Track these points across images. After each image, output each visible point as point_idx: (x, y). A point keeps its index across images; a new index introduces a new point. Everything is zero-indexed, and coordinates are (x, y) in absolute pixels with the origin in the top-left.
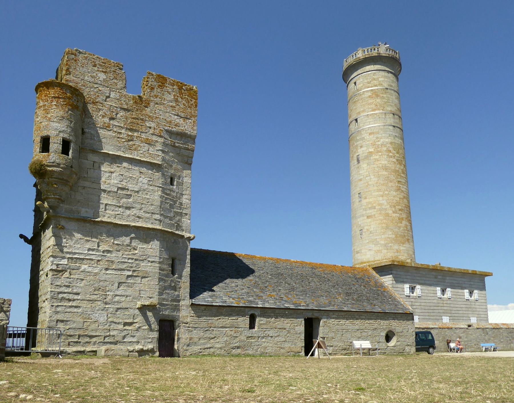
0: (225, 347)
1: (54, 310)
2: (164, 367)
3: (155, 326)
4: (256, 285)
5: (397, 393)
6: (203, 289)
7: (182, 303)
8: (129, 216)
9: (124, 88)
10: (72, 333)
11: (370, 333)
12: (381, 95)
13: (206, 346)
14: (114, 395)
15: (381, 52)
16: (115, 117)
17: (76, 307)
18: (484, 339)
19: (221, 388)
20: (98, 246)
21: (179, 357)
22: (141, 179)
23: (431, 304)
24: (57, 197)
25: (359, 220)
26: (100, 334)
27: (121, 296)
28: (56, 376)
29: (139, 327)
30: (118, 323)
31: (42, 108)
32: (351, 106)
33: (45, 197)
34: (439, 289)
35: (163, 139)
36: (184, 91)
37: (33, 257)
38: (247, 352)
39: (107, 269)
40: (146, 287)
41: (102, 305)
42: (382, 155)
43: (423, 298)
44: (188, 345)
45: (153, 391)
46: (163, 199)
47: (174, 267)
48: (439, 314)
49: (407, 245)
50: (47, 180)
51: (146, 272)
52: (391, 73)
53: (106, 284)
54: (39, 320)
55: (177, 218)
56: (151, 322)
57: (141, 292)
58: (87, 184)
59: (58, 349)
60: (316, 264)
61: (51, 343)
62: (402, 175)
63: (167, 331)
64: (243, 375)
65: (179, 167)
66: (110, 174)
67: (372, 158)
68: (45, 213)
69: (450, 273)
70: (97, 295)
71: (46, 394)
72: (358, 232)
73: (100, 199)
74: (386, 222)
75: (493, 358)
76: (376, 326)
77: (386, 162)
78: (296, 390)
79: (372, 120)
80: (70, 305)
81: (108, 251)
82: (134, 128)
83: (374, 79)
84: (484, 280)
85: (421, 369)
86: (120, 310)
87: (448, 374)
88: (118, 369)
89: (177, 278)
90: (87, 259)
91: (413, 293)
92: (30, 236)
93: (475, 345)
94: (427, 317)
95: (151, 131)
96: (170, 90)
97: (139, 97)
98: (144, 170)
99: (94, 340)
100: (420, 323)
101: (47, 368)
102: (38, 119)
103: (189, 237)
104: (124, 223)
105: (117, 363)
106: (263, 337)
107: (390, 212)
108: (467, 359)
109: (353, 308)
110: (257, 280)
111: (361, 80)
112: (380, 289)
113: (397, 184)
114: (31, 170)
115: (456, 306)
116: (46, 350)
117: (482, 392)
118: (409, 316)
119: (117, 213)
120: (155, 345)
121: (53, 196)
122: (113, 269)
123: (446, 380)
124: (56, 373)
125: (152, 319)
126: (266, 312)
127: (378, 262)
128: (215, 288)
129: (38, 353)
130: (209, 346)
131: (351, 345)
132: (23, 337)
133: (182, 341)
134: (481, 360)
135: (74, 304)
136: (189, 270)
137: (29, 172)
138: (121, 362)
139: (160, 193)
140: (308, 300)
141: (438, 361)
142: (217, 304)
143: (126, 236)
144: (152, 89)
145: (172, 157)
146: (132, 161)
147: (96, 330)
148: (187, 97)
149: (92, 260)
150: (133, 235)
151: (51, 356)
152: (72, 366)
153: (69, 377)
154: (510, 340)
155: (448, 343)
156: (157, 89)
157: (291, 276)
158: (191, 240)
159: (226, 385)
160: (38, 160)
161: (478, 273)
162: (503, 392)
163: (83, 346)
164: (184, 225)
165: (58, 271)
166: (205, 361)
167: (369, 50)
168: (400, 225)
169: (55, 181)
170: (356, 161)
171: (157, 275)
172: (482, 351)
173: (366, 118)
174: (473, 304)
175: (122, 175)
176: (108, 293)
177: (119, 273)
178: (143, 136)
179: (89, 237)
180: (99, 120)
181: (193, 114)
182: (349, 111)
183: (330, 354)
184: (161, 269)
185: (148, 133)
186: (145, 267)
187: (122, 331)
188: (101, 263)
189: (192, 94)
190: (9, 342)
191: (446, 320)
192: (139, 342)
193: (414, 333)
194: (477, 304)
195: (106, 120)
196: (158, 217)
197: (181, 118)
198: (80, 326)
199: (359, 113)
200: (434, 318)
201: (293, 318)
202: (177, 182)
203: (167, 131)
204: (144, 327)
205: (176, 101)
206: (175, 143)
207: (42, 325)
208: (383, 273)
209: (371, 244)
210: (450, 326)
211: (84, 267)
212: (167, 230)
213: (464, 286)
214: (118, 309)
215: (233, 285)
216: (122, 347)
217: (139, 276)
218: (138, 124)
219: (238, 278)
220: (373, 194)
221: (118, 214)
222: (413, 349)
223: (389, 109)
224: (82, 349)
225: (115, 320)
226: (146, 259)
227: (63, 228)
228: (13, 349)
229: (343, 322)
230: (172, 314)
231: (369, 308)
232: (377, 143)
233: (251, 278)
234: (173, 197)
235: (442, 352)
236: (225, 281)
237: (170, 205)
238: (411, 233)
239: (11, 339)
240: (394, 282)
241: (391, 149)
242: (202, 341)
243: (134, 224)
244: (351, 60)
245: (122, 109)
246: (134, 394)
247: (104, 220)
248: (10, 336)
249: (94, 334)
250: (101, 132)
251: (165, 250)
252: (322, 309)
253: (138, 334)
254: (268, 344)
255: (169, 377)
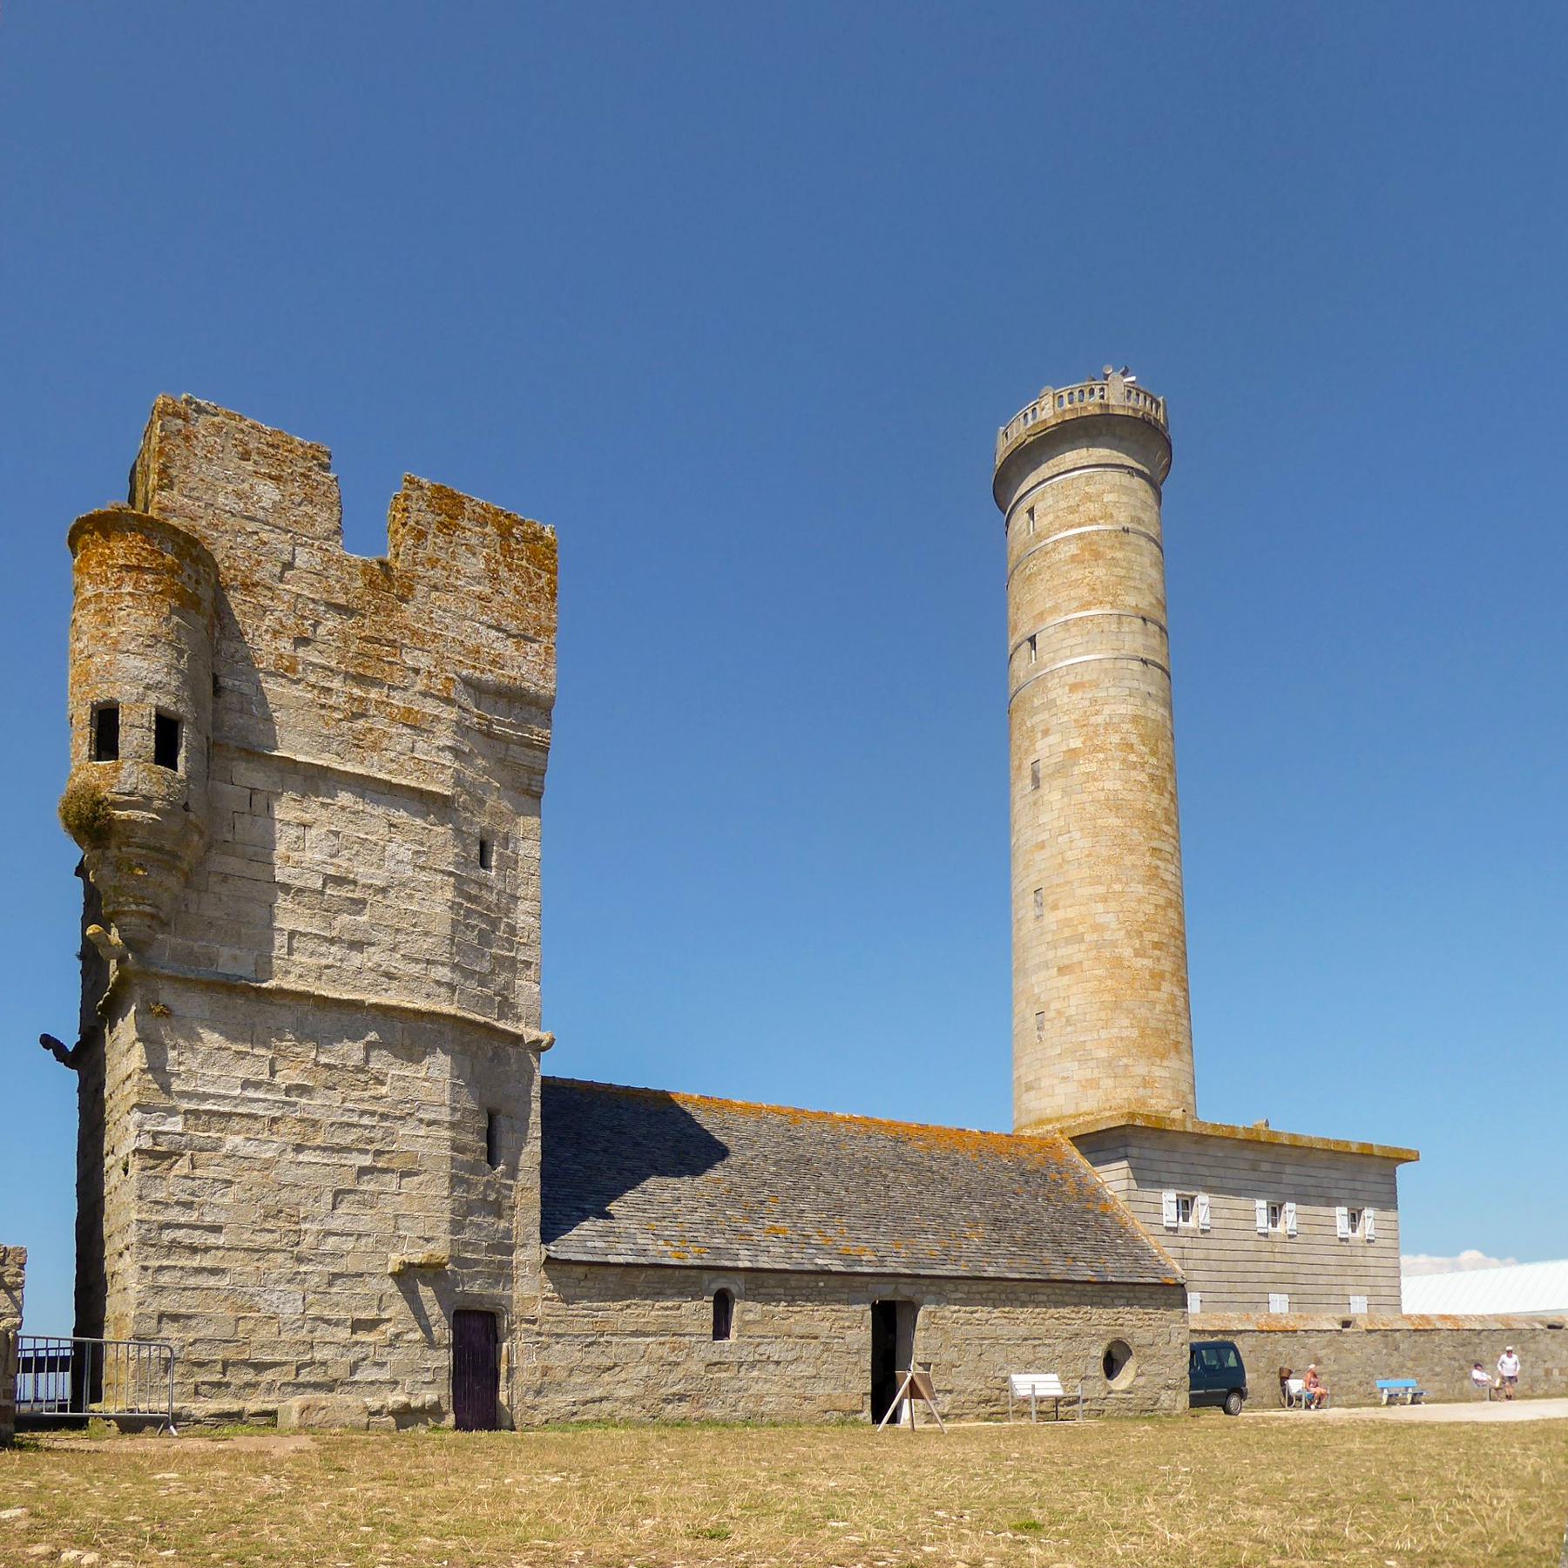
0: (642, 1397)
1: (148, 1280)
2: (471, 1460)
3: (443, 1331)
4: (733, 1196)
5: (1134, 1539)
6: (578, 1209)
7: (519, 1256)
8: (359, 971)
9: (336, 533)
10: (204, 1357)
11: (1059, 1349)
12: (1109, 554)
13: (589, 1395)
14: (330, 1549)
15: (1112, 402)
16: (309, 634)
17: (213, 1272)
18: (1387, 1366)
19: (633, 1525)
20: (273, 1073)
21: (513, 1429)
22: (392, 848)
23: (1239, 1256)
24: (148, 909)
25: (1034, 979)
26: (284, 1359)
27: (342, 1235)
28: (163, 1493)
29: (397, 1336)
30: (337, 1324)
31: (92, 607)
32: (1018, 593)
33: (110, 909)
34: (1262, 1204)
35: (455, 710)
36: (518, 542)
37: (82, 1108)
38: (707, 1411)
39: (299, 1148)
41: (289, 1264)
42: (1106, 759)
43: (1215, 1233)
44: (538, 1393)
45: (441, 1537)
46: (458, 914)
47: (493, 1142)
48: (1258, 1288)
49: (1173, 1062)
50: (115, 851)
51: (415, 1158)
52: (1141, 474)
53: (295, 1198)
54: (109, 1314)
55: (502, 978)
56: (432, 1319)
57: (400, 1220)
58: (232, 864)
59: (164, 1406)
60: (908, 1126)
61: (144, 1388)
62: (1166, 828)
63: (476, 1343)
64: (695, 1484)
65: (505, 805)
66: (300, 832)
67: (1076, 770)
68: (113, 963)
69: (1296, 1152)
70: (272, 1231)
71: (136, 1548)
72: (1032, 1021)
73: (272, 918)
74: (1115, 985)
75: (1411, 1425)
76: (1077, 1325)
77: (1118, 785)
78: (846, 1532)
79: (1079, 640)
80: (195, 1264)
81: (303, 1090)
82: (369, 673)
83: (1089, 498)
84: (1393, 1176)
85: (1204, 1462)
86: (339, 1282)
87: (1279, 1475)
88: (340, 1470)
89: (503, 1175)
90: (242, 1115)
91: (1186, 1219)
92: (71, 1040)
93: (1360, 1384)
94: (1225, 1297)
95: (421, 684)
96: (474, 541)
97: (382, 563)
98: (400, 816)
99: (268, 1376)
100: (1203, 1316)
101: (137, 1467)
102: (81, 645)
103: (539, 1041)
104: (345, 997)
105: (335, 1449)
106: (753, 1365)
107: (1127, 952)
108: (1336, 1430)
109: (1011, 1269)
110: (736, 1180)
111: (1050, 501)
112: (1090, 1205)
113: (1148, 859)
114: (65, 818)
115: (1312, 1259)
116: (132, 1411)
117: (1374, 1532)
118: (1172, 1294)
119: (324, 962)
120: (443, 1393)
121: (134, 907)
122: (318, 1147)
123: (1272, 1496)
124: (164, 1483)
125: (434, 1310)
126: (764, 1284)
127: (1088, 1118)
128: (613, 1207)
129: (108, 1418)
130: (598, 1393)
131: (1005, 1386)
132: (64, 1369)
133: (521, 1378)
134: (1375, 1431)
135: (207, 1261)
136: (539, 1149)
137: (61, 825)
138: (347, 1445)
139: (449, 894)
140: (883, 1243)
141: (1253, 1437)
142: (621, 1260)
143: (354, 1039)
144: (421, 535)
145: (485, 771)
146: (364, 786)
147: (273, 1346)
148: (524, 563)
149: (254, 1117)
150: (373, 1036)
151: (148, 1429)
152: (208, 1462)
153: (199, 1496)
154: (1461, 1368)
155: (1283, 1380)
156: (435, 536)
157: (834, 1166)
158: (544, 1049)
159: (647, 1516)
160: (85, 786)
161: (1376, 1152)
162: (1435, 1531)
163: (236, 1396)
164: (521, 1001)
165: (158, 1156)
166: (587, 1442)
167: (1076, 394)
168: (1153, 994)
169: (141, 856)
170: (1028, 781)
171: (446, 1167)
172: (1378, 1404)
173: (1062, 635)
174: (1360, 1252)
175: (336, 834)
176: (304, 1226)
177: (335, 1159)
178: (397, 699)
179: (244, 1041)
180: (262, 645)
181: (545, 623)
182: (1011, 610)
183: (943, 1416)
185: (411, 692)
186: (415, 1139)
187: (347, 1347)
188: (281, 1127)
189: (542, 553)
190: (26, 1384)
191: (1279, 1304)
192: (396, 1383)
193: (1187, 1348)
194: (1371, 1252)
195: (285, 645)
196: (443, 973)
197: (510, 636)
198: (227, 1331)
199: (1041, 616)
200: (1246, 1298)
201: (838, 1302)
202: (500, 855)
203: (467, 682)
204: (411, 1336)
205: (494, 577)
206: (491, 722)
207: (118, 1330)
208: (1101, 1155)
209: (1070, 1060)
210: (1292, 1325)
211: (232, 1141)
212: (471, 1016)
213: (1335, 1193)
214: (336, 1276)
215: (667, 1196)
216: (349, 1399)
217: (393, 1171)
218: (380, 659)
219: (679, 1175)
220: (1079, 891)
221: (327, 967)
222: (1183, 1399)
223: (1131, 600)
224: (235, 1406)
225: (327, 1313)
226: (411, 1115)
227: (167, 1013)
228: (37, 1407)
229: (982, 1313)
230: (491, 1291)
231: (1058, 1270)
232: (1093, 720)
233: (716, 1173)
234: (488, 908)
235: (1265, 1406)
236: (644, 1185)
237: (481, 933)
238: (1185, 1022)
239: (30, 1376)
240: (1134, 1184)
241: (1134, 739)
242: (578, 1379)
243: (374, 999)
244: (1019, 430)
245: (331, 606)
246: (386, 1546)
247: (286, 986)
248: (27, 1365)
249: (269, 1359)
250: (271, 686)
251: (468, 1085)
252: (922, 1272)
253: (393, 1358)
254: (768, 1386)
255: (485, 1493)
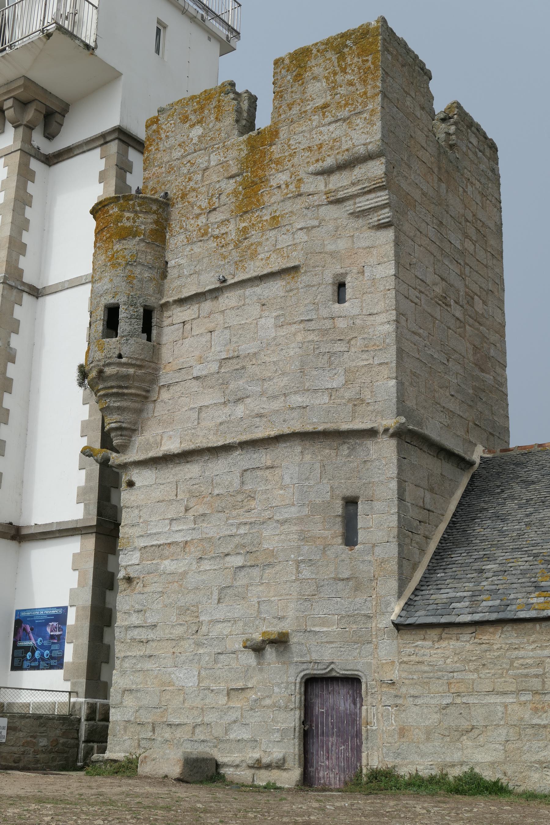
26: (186, 721)
40: (272, 593)
184: (304, 538)
221: (221, 424)
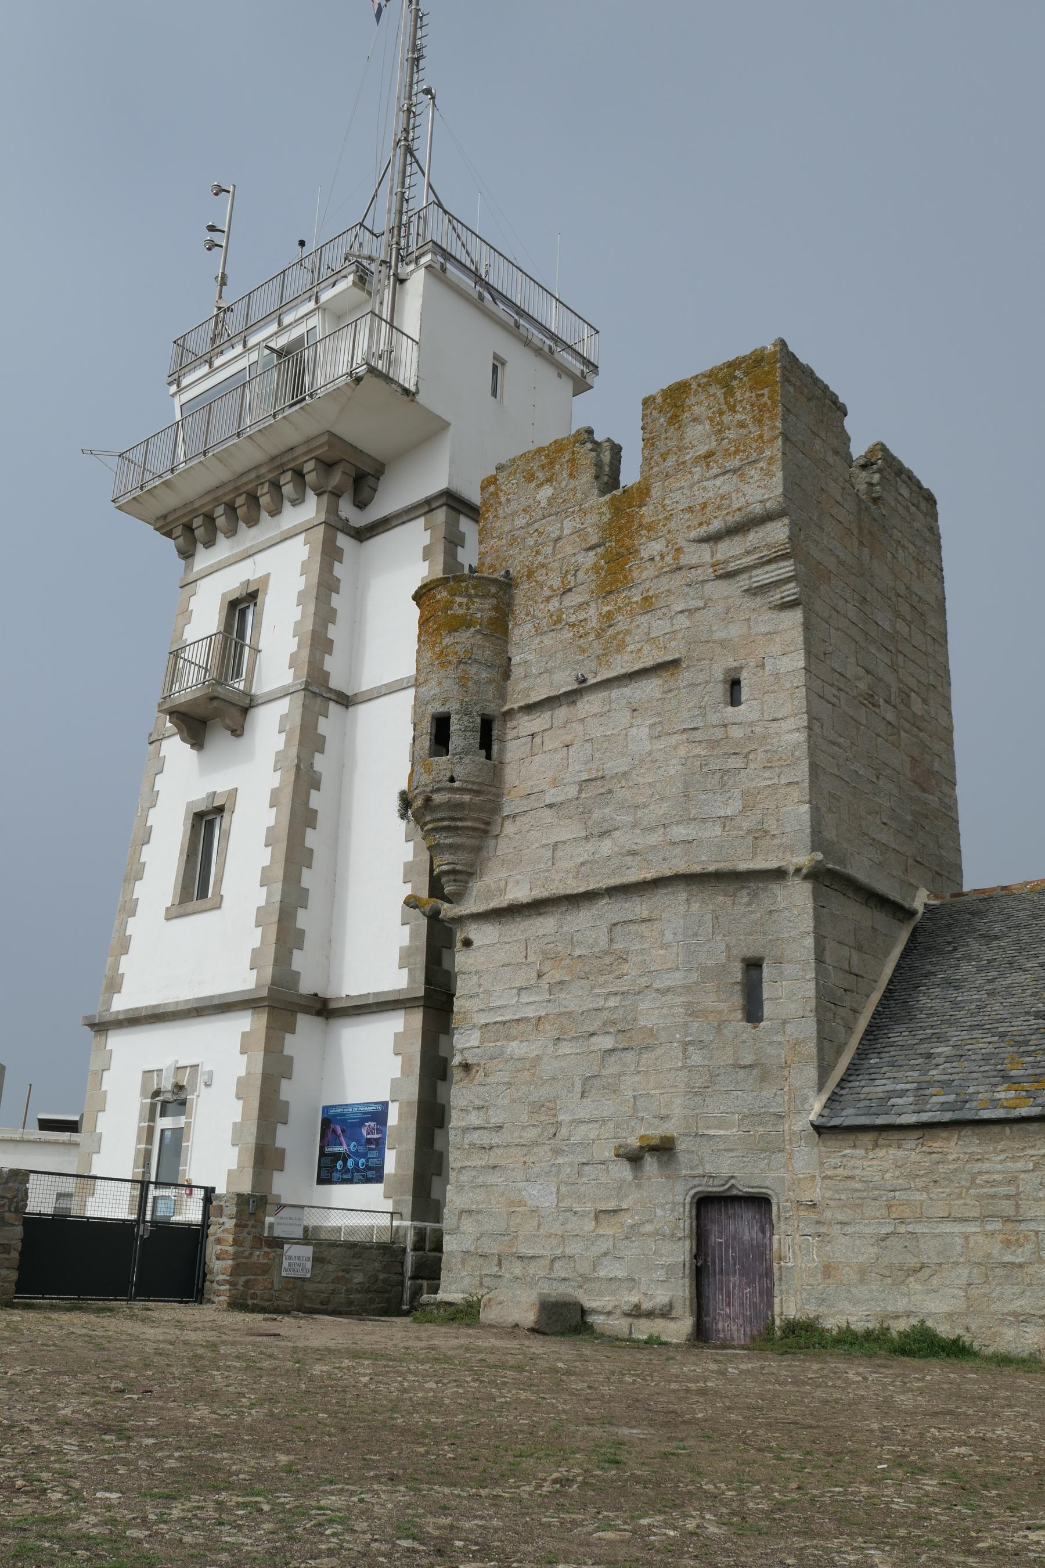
26: (541, 1252)
51: (651, 1032)
135: (492, 1159)
221: (582, 864)
